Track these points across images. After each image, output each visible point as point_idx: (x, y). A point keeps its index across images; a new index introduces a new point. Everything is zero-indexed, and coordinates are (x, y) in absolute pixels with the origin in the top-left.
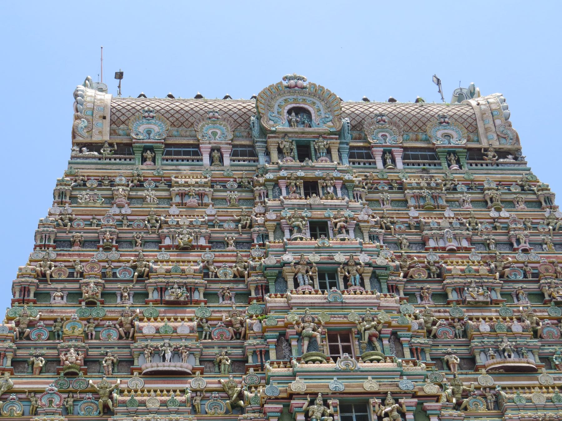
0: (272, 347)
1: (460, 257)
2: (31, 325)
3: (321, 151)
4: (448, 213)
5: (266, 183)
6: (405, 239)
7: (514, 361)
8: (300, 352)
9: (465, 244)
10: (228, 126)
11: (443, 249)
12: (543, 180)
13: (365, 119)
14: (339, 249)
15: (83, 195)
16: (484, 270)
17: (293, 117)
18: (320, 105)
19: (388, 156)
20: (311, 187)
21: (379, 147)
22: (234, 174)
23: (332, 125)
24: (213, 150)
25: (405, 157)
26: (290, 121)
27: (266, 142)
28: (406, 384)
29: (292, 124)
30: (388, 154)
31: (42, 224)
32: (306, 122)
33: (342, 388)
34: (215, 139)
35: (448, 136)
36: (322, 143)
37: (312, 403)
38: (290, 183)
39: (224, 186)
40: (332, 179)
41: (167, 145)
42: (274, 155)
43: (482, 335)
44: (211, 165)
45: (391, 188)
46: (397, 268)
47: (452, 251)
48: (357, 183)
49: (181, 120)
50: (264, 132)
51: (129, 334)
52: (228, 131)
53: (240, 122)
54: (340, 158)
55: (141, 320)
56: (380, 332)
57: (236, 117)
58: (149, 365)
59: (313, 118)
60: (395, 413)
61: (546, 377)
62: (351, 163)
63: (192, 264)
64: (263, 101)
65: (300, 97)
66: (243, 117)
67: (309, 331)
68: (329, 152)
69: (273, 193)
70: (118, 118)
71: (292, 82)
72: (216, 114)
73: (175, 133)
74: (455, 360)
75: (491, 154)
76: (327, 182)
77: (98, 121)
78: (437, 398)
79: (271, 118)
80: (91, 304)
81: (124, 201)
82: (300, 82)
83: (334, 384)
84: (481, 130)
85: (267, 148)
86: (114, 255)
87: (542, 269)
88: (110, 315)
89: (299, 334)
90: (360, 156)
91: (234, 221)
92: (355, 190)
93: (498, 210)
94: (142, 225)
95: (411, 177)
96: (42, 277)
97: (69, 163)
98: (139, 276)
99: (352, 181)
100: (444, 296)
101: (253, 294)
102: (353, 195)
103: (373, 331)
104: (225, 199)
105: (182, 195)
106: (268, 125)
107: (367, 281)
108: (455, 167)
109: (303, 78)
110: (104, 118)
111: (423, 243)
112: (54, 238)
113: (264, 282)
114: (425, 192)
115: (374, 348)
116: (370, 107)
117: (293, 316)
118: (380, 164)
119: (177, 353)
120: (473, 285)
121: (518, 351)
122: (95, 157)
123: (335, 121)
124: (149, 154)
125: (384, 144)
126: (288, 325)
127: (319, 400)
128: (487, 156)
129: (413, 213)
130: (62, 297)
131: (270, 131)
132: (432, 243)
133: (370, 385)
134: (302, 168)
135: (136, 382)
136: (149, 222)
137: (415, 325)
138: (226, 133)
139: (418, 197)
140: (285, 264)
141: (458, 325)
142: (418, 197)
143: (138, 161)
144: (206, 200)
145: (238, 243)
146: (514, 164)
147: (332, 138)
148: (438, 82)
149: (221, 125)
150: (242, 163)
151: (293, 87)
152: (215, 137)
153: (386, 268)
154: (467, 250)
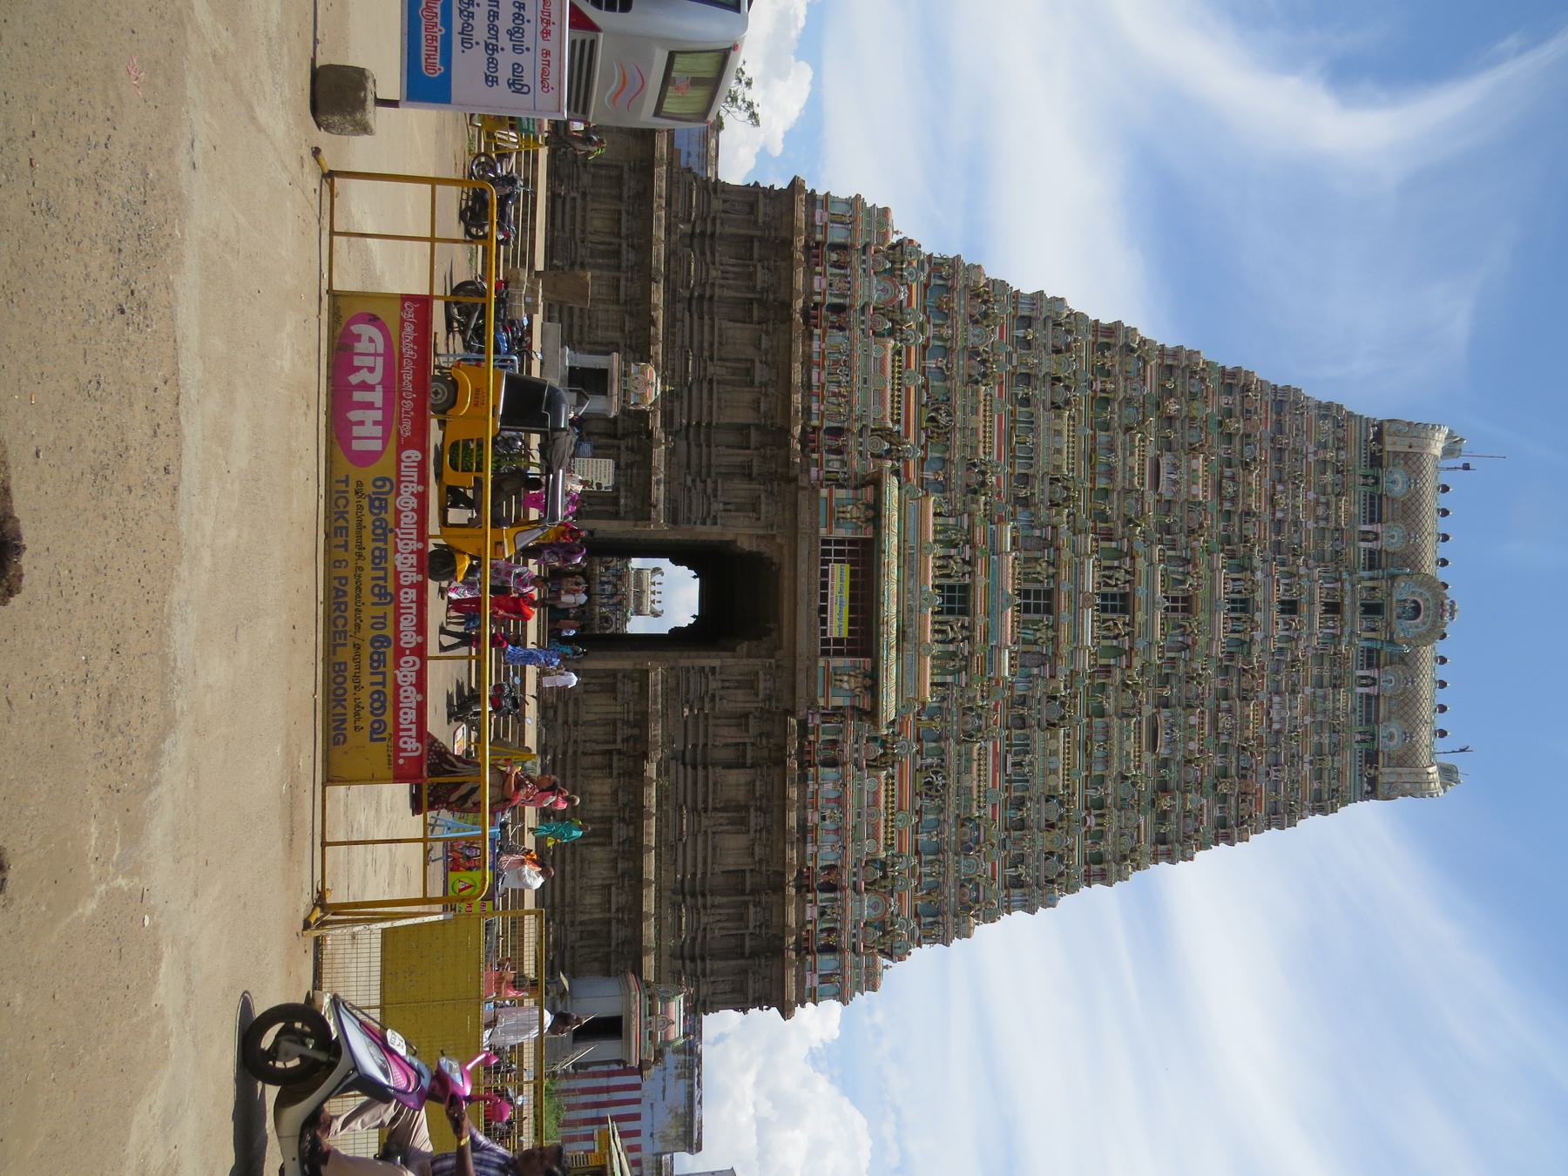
2: (1203, 380)
4: (1308, 720)
6: (1282, 677)
7: (1162, 737)
9: (1276, 726)
15: (1327, 425)
18: (1423, 629)
20: (1333, 608)
24: (1376, 534)
25: (1368, 696)
28: (1140, 644)
31: (1297, 391)
33: (1139, 594)
35: (1391, 737)
37: (1127, 572)
41: (1380, 497)
42: (1370, 584)
43: (1186, 717)
49: (1409, 510)
50: (1393, 577)
51: (1193, 450)
54: (1367, 639)
55: (1205, 460)
58: (1164, 462)
68: (1374, 630)
70: (1412, 460)
74: (1166, 692)
77: (1407, 441)
81: (1321, 455)
83: (1141, 592)
84: (1399, 770)
86: (1267, 445)
90: (1369, 658)
93: (1311, 763)
95: (1345, 700)
96: (1246, 388)
100: (1226, 699)
105: (1327, 505)
107: (1237, 635)
108: (1358, 737)
111: (1278, 693)
112: (1284, 400)
114: (1329, 705)
119: (1175, 482)
126: (1195, 566)
127: (1128, 577)
129: (1308, 690)
132: (1276, 699)
133: (1140, 617)
135: (1151, 452)
142: (1325, 698)
143: (1362, 471)
144: (1322, 524)
151: (1442, 609)
153: (1249, 653)
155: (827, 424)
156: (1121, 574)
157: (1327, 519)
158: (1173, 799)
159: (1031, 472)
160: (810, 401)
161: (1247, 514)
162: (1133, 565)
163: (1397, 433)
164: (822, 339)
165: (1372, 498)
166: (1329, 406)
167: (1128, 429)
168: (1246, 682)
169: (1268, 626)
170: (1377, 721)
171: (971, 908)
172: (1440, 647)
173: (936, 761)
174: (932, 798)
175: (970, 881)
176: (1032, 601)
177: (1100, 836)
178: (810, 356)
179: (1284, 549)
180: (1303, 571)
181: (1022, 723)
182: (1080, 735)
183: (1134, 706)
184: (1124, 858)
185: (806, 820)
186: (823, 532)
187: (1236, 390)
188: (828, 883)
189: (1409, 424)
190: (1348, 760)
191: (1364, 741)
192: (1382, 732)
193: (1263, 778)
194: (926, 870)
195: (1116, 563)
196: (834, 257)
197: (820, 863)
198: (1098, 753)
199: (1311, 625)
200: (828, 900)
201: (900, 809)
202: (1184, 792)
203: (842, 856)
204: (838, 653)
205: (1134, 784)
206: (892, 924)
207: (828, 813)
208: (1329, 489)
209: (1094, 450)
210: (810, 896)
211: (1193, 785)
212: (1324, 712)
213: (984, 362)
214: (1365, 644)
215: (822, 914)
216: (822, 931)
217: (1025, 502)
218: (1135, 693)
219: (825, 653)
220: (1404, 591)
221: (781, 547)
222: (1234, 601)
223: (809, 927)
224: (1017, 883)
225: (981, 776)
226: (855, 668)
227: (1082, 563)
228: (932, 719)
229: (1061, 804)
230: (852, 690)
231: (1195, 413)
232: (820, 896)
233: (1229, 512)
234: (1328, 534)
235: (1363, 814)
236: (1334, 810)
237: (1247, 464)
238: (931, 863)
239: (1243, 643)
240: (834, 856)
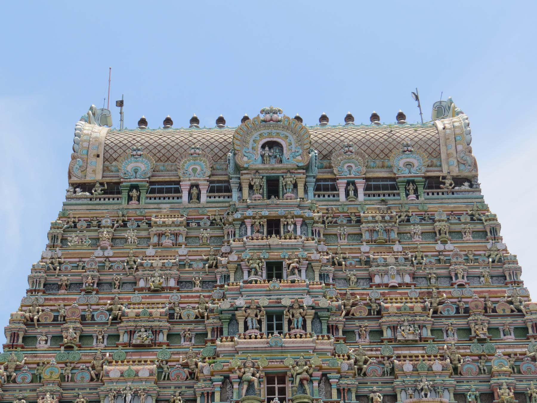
0: (217, 390)
1: (400, 294)
2: (17, 369)
3: (288, 187)
4: (397, 247)
5: (234, 222)
6: (352, 275)
9: (408, 279)
10: (207, 162)
11: (386, 285)
12: (493, 210)
13: (336, 148)
14: (283, 294)
15: (73, 238)
16: (418, 307)
17: (267, 151)
18: (292, 138)
19: (351, 187)
20: (274, 226)
21: (344, 178)
22: (208, 211)
23: (301, 159)
24: (192, 186)
25: (368, 188)
26: (263, 156)
27: (239, 178)
29: (265, 158)
30: (351, 185)
32: (278, 156)
34: (194, 176)
35: (409, 165)
36: (289, 180)
38: (255, 222)
39: (198, 224)
40: (293, 218)
41: (152, 183)
42: (246, 190)
43: (405, 375)
44: (189, 202)
45: (350, 221)
46: (339, 308)
47: (393, 287)
48: (317, 219)
49: (166, 155)
50: (238, 168)
51: (98, 377)
52: (206, 168)
53: (221, 155)
54: (306, 191)
56: (311, 376)
57: (216, 150)
59: (285, 152)
62: (317, 196)
64: (239, 137)
65: (274, 131)
66: (223, 150)
67: (248, 376)
68: (295, 186)
69: (240, 231)
70: (111, 155)
71: (268, 117)
72: (197, 151)
73: (161, 168)
75: (448, 182)
76: (288, 220)
77: (92, 160)
79: (245, 154)
80: (69, 348)
82: (275, 115)
84: (443, 156)
85: (240, 184)
86: (93, 298)
87: (471, 305)
88: (84, 359)
89: (240, 378)
90: (326, 189)
91: (202, 260)
92: (314, 227)
93: (444, 242)
94: (121, 268)
96: (29, 322)
97: (64, 205)
98: (113, 319)
99: (312, 218)
100: (381, 332)
101: (209, 336)
102: (312, 231)
103: (305, 375)
104: (198, 237)
105: (160, 235)
106: (243, 161)
108: (412, 196)
109: (279, 111)
110: (98, 156)
111: (370, 279)
112: (45, 282)
113: (219, 325)
114: (379, 226)
115: (304, 392)
116: (342, 136)
117: (235, 362)
118: (342, 197)
120: (406, 323)
122: (86, 198)
123: (303, 156)
124: (134, 193)
125: (348, 176)
126: (231, 371)
128: (444, 183)
129: (365, 248)
130: (46, 341)
131: (243, 167)
132: (377, 280)
134: (267, 206)
136: (128, 262)
138: (205, 170)
139: (372, 231)
140: (237, 309)
141: (387, 363)
142: (372, 231)
143: (124, 201)
144: (181, 239)
145: (203, 282)
146: (469, 191)
147: (300, 173)
148: (417, 98)
149: (201, 161)
150: (217, 199)
151: (270, 120)
152: (194, 174)
153: (328, 310)
154: (408, 285)
157: (177, 235)
158: (500, 386)
161: (171, 316)
163: (84, 170)
165: (153, 191)
166: (53, 238)
168: (361, 312)
169: (296, 292)
170: (394, 179)
172: (310, 121)
179: (210, 277)
180: (234, 257)
187: (31, 332)
189: (74, 158)
190: (438, 205)
191: (416, 191)
192: (404, 174)
193: (467, 291)
199: (294, 248)
202: (491, 374)
208: (144, 234)
211: (482, 364)
212: (387, 231)
220: (252, 157)
222: (270, 328)
233: (169, 336)
234: (193, 233)
235: (496, 189)
236: (494, 218)
237: (115, 318)
239: (317, 317)
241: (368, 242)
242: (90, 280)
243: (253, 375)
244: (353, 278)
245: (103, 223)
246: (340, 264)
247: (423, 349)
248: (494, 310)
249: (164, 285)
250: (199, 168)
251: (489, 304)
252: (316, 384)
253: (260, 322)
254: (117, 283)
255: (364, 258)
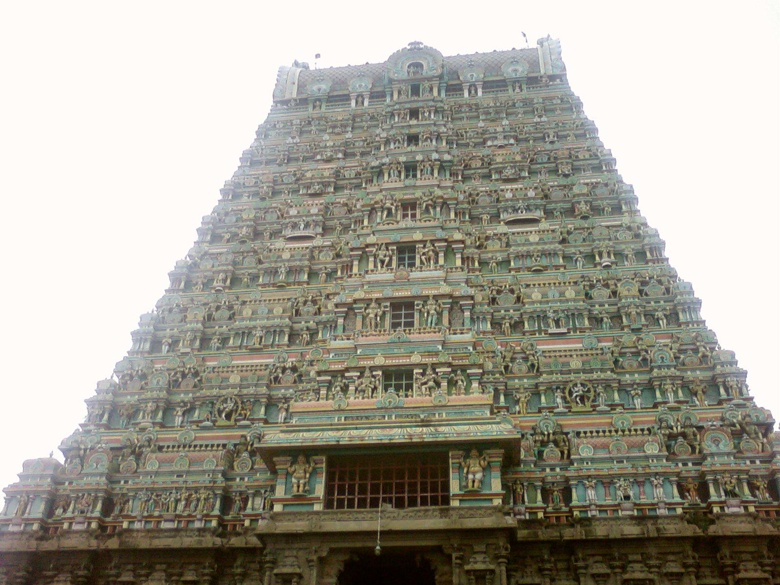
8: (382, 218)
9: (512, 141)
11: (496, 146)
24: (358, 96)
35: (516, 71)
56: (435, 202)
58: (289, 233)
60: (431, 253)
61: (544, 225)
63: (327, 170)
67: (388, 205)
71: (413, 46)
78: (463, 242)
86: (284, 168)
89: (382, 207)
90: (455, 90)
93: (540, 117)
103: (430, 202)
108: (517, 90)
117: (379, 197)
118: (466, 94)
120: (509, 168)
121: (528, 209)
126: (376, 203)
127: (383, 247)
129: (481, 124)
133: (418, 236)
137: (461, 197)
140: (384, 164)
143: (310, 108)
148: (525, 35)
155: (216, 512)
156: (381, 254)
158: (579, 203)
159: (287, 330)
160: (192, 530)
162: (373, 245)
164: (132, 519)
165: (330, 102)
167: (260, 262)
170: (504, 81)
171: (704, 356)
173: (559, 394)
174: (597, 395)
175: (677, 358)
176: (403, 320)
177: (620, 255)
178: (149, 531)
181: (517, 326)
182: (526, 277)
183: (500, 239)
184: (637, 236)
185: (632, 518)
186: (318, 507)
188: (697, 490)
191: (520, 87)
193: (557, 145)
194: (671, 397)
195: (371, 259)
196: (59, 511)
197: (678, 499)
198: (545, 262)
200: (717, 490)
201: (611, 424)
203: (666, 476)
204: (446, 487)
205: (569, 233)
206: (734, 425)
207: (620, 493)
209: (274, 285)
210: (716, 509)
213: (184, 375)
214: (443, 94)
215: (735, 495)
216: (754, 495)
217: (313, 333)
218: (487, 238)
219: (446, 500)
221: (332, 551)
223: (752, 509)
224: (673, 317)
225: (568, 349)
226: (460, 468)
227: (369, 282)
228: (517, 402)
229: (592, 286)
230: (484, 469)
231: (252, 216)
232: (714, 497)
238: (664, 393)
240: (668, 485)
241: (483, 120)
242: (282, 157)
243: (392, 204)
244: (471, 144)
245: (294, 122)
246: (462, 136)
247: (522, 184)
248: (577, 157)
249: (334, 157)
250: (363, 85)
251: (573, 152)
252: (438, 209)
253: (400, 172)
254: (301, 158)
255: (480, 131)
